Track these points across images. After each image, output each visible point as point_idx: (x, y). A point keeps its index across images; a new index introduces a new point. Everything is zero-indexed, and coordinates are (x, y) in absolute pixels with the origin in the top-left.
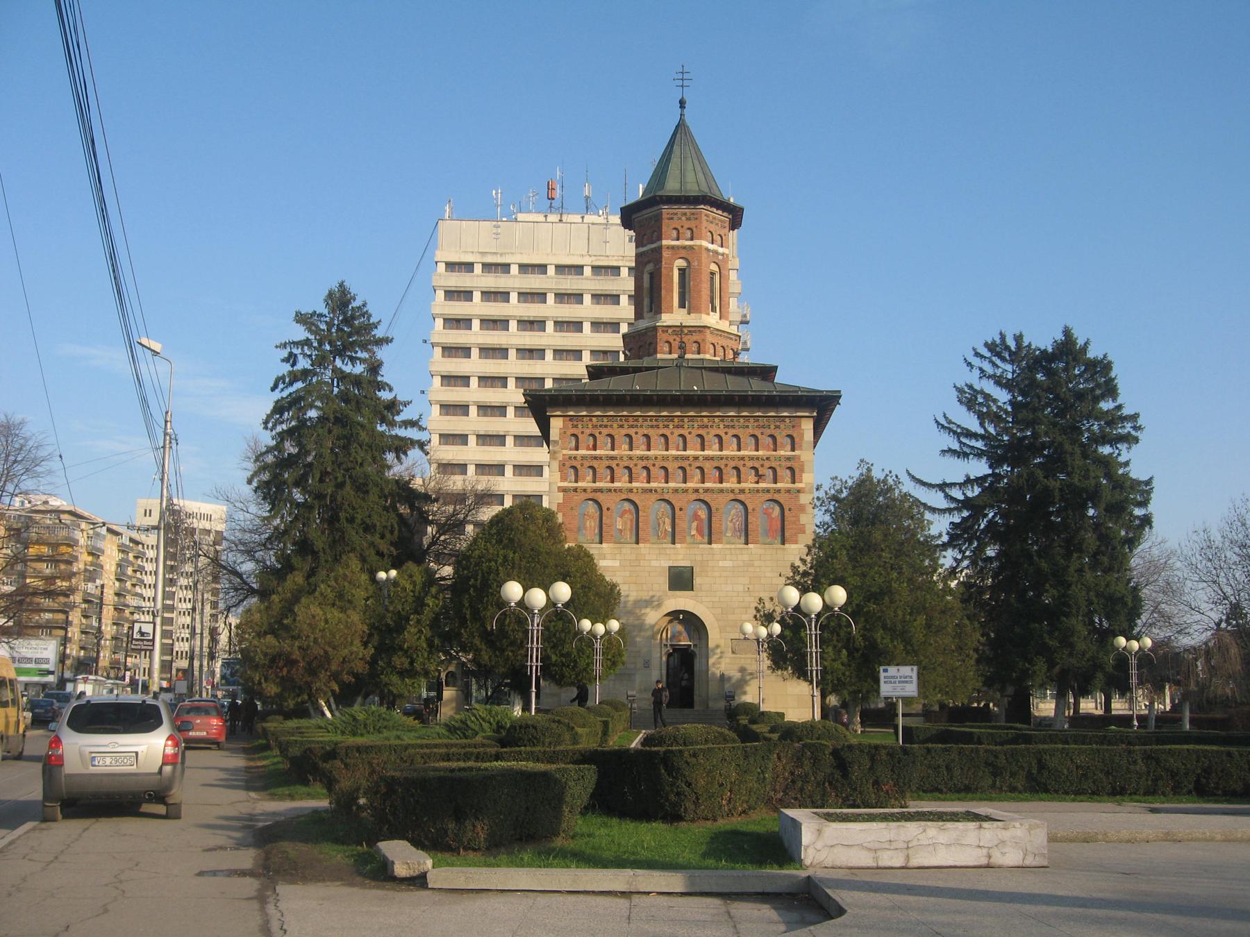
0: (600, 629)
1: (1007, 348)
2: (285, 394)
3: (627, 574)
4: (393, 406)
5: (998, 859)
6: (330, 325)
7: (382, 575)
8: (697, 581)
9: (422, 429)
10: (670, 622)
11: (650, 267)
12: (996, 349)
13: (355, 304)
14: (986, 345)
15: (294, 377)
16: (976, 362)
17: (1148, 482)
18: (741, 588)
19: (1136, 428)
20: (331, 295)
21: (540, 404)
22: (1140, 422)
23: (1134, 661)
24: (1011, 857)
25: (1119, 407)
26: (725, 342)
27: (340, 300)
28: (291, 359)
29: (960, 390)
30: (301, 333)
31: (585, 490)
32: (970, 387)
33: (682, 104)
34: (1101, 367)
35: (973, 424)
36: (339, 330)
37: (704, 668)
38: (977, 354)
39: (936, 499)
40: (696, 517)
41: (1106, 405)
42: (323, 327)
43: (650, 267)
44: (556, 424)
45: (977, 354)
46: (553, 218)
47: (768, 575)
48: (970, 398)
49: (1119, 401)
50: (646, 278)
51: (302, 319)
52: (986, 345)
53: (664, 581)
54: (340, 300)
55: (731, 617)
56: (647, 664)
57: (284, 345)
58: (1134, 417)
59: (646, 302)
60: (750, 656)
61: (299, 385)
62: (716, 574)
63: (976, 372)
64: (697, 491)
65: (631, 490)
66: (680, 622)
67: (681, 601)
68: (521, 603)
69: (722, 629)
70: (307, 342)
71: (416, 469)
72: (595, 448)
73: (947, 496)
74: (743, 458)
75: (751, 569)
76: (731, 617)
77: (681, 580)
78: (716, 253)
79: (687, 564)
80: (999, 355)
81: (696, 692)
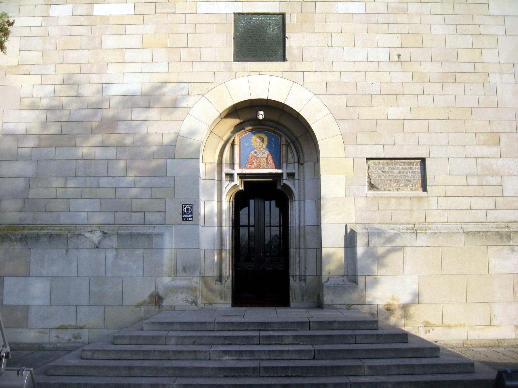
3: (150, 29)
8: (293, 41)
10: (238, 128)
18: (383, 55)
37: (310, 221)
47: (438, 29)
53: (225, 42)
55: (366, 113)
56: (188, 213)
60: (407, 192)
62: (332, 28)
66: (258, 127)
67: (262, 81)
69: (348, 139)
75: (402, 18)
76: (366, 113)
79: (273, 8)
81: (294, 270)
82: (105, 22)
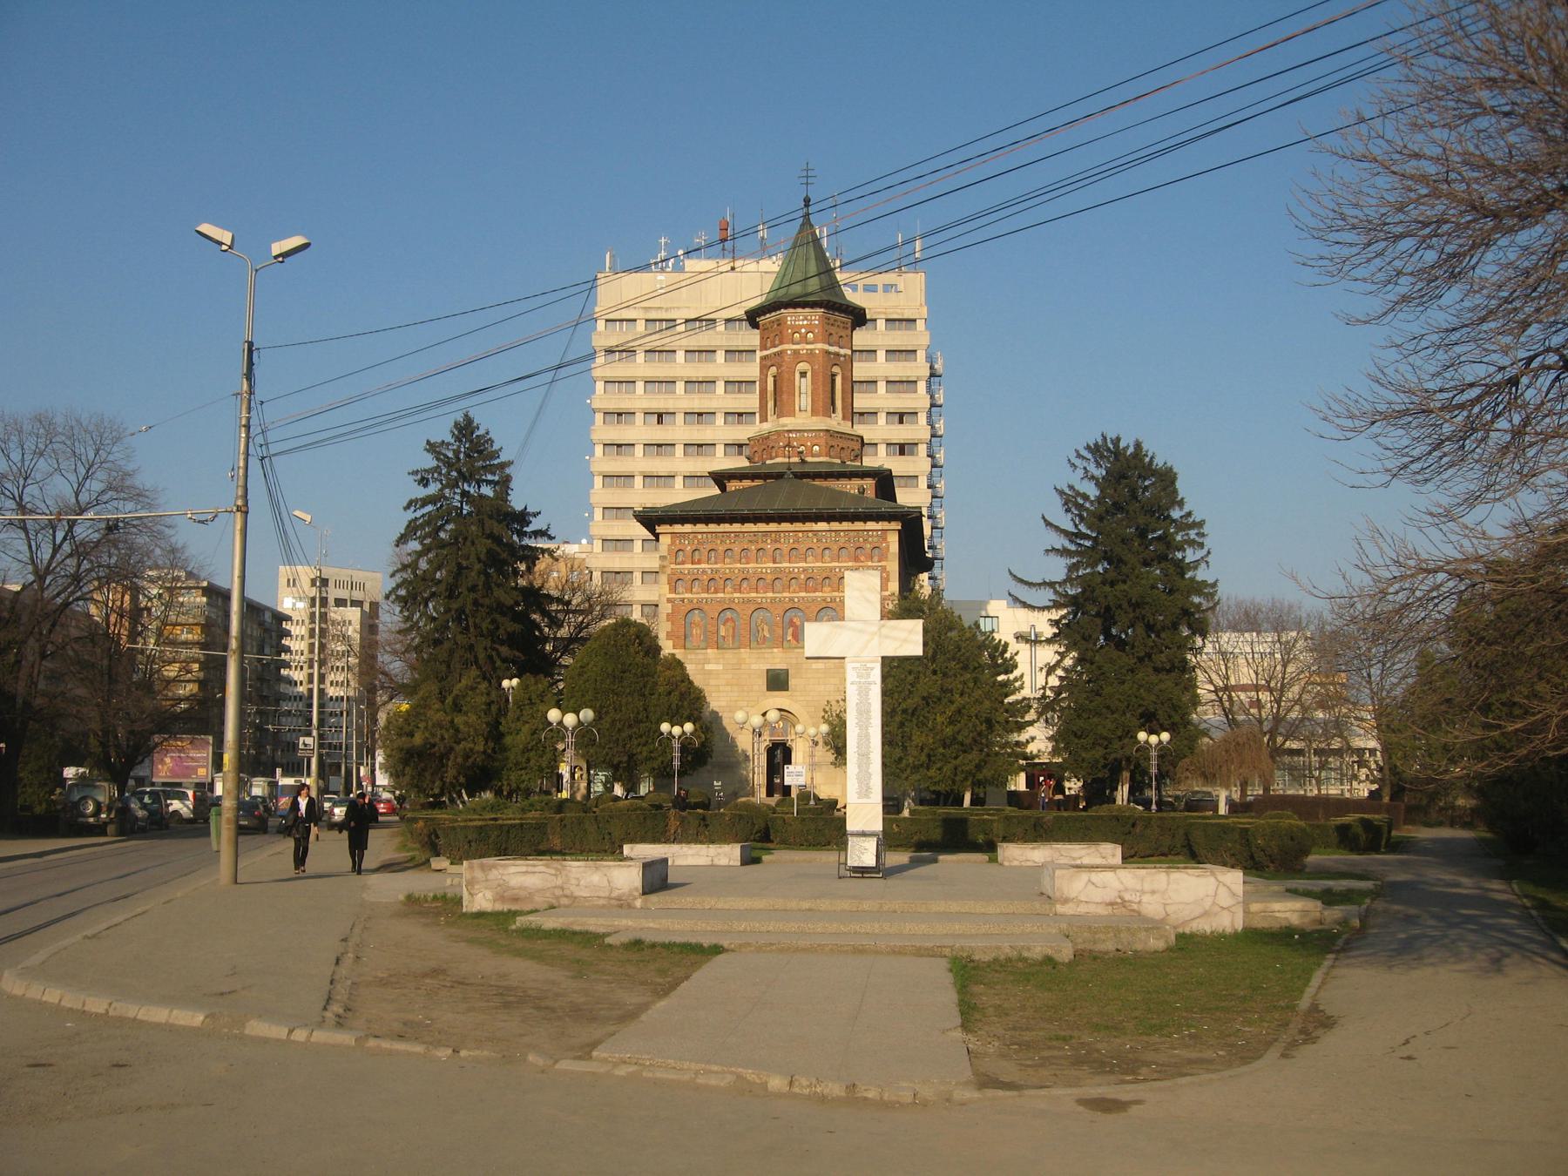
0: (677, 730)
1: (1108, 450)
2: (419, 514)
4: (523, 517)
5: (717, 862)
6: (456, 453)
7: (506, 683)
8: (792, 682)
9: (551, 538)
11: (773, 370)
12: (1096, 450)
13: (481, 432)
14: (1088, 447)
15: (425, 502)
16: (1078, 462)
17: (1214, 585)
19: (1203, 535)
20: (456, 424)
21: (651, 520)
22: (1205, 530)
23: (1154, 753)
24: (723, 861)
25: (1189, 514)
26: (844, 444)
27: (465, 429)
28: (424, 482)
29: (1061, 493)
30: (429, 462)
31: (691, 601)
32: (1071, 487)
33: (807, 202)
34: (1167, 478)
35: (1066, 523)
36: (467, 456)
38: (1079, 456)
39: (1047, 596)
40: (792, 623)
41: (1176, 514)
42: (450, 455)
43: (773, 370)
44: (665, 540)
45: (1079, 456)
46: (725, 265)
48: (1071, 500)
49: (1186, 509)
50: (770, 381)
51: (432, 447)
52: (1088, 447)
53: (763, 682)
54: (465, 429)
57: (415, 473)
58: (1200, 524)
59: (770, 404)
61: (430, 508)
63: (1080, 473)
64: (791, 599)
65: (732, 600)
68: (560, 723)
70: (437, 469)
71: (550, 576)
72: (699, 562)
73: (1056, 592)
74: (831, 569)
77: (777, 681)
78: (837, 354)
79: (784, 667)
80: (1102, 457)
82: (710, 672)
